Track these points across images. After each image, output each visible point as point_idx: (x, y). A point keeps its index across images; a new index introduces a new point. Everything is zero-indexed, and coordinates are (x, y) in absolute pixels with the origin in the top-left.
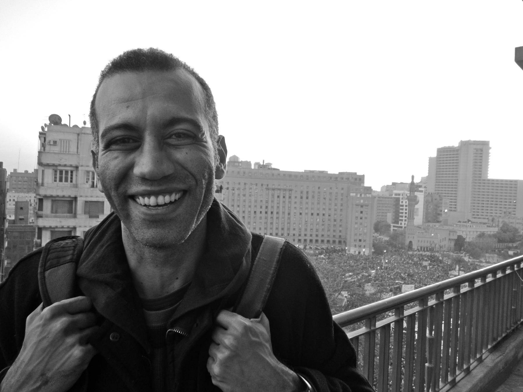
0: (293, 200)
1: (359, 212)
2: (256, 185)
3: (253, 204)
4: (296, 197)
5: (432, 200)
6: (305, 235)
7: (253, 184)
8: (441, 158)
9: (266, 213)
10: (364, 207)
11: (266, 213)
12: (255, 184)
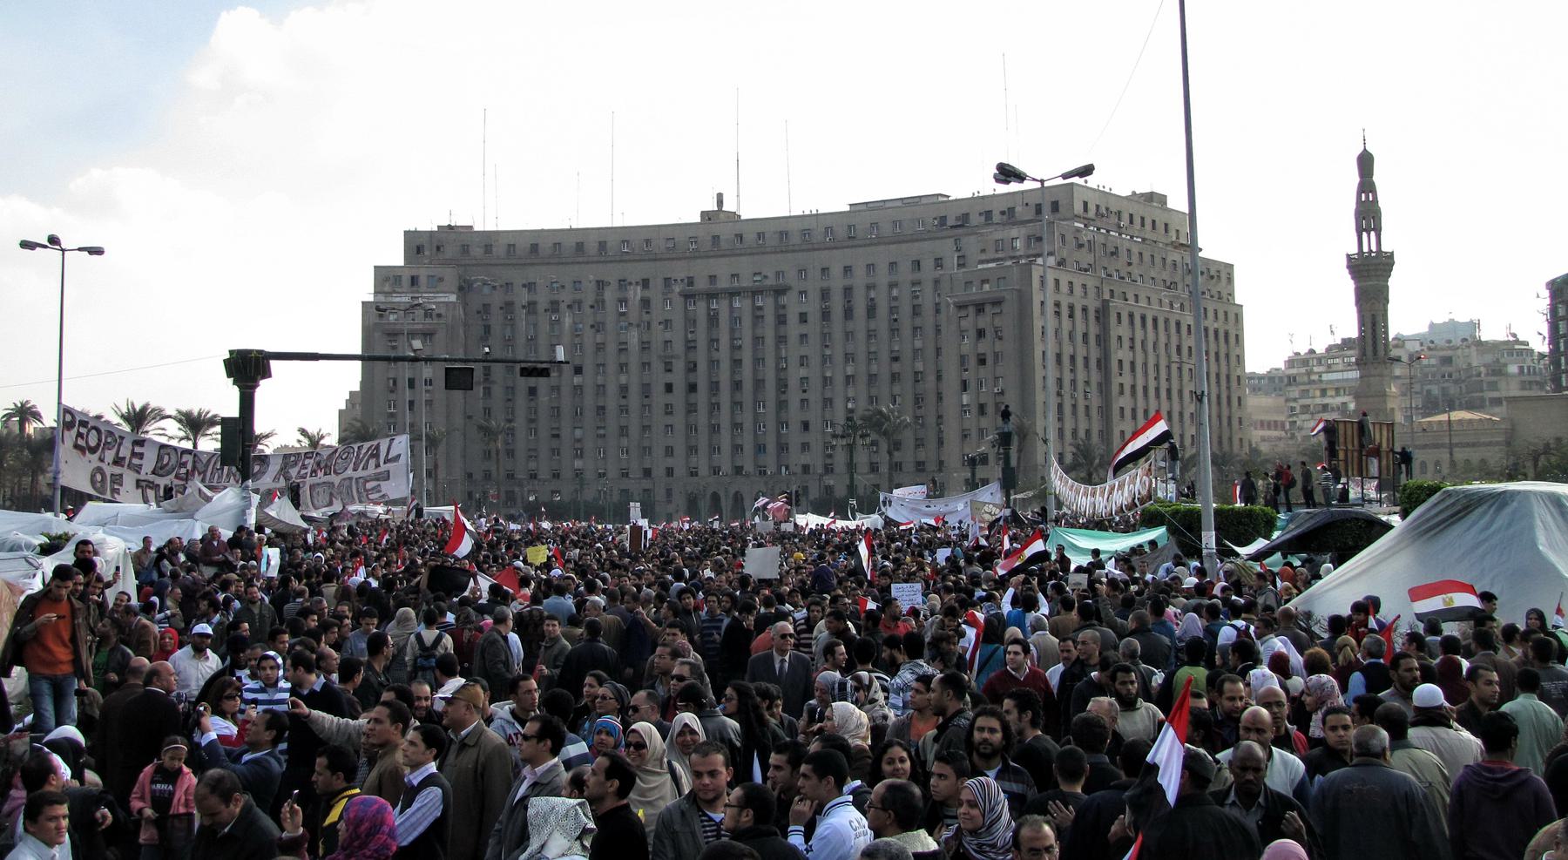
0: (793, 329)
1: (973, 333)
2: (645, 283)
3: (634, 360)
4: (803, 318)
7: (630, 284)
9: (692, 388)
10: (988, 308)
11: (692, 388)
12: (637, 283)
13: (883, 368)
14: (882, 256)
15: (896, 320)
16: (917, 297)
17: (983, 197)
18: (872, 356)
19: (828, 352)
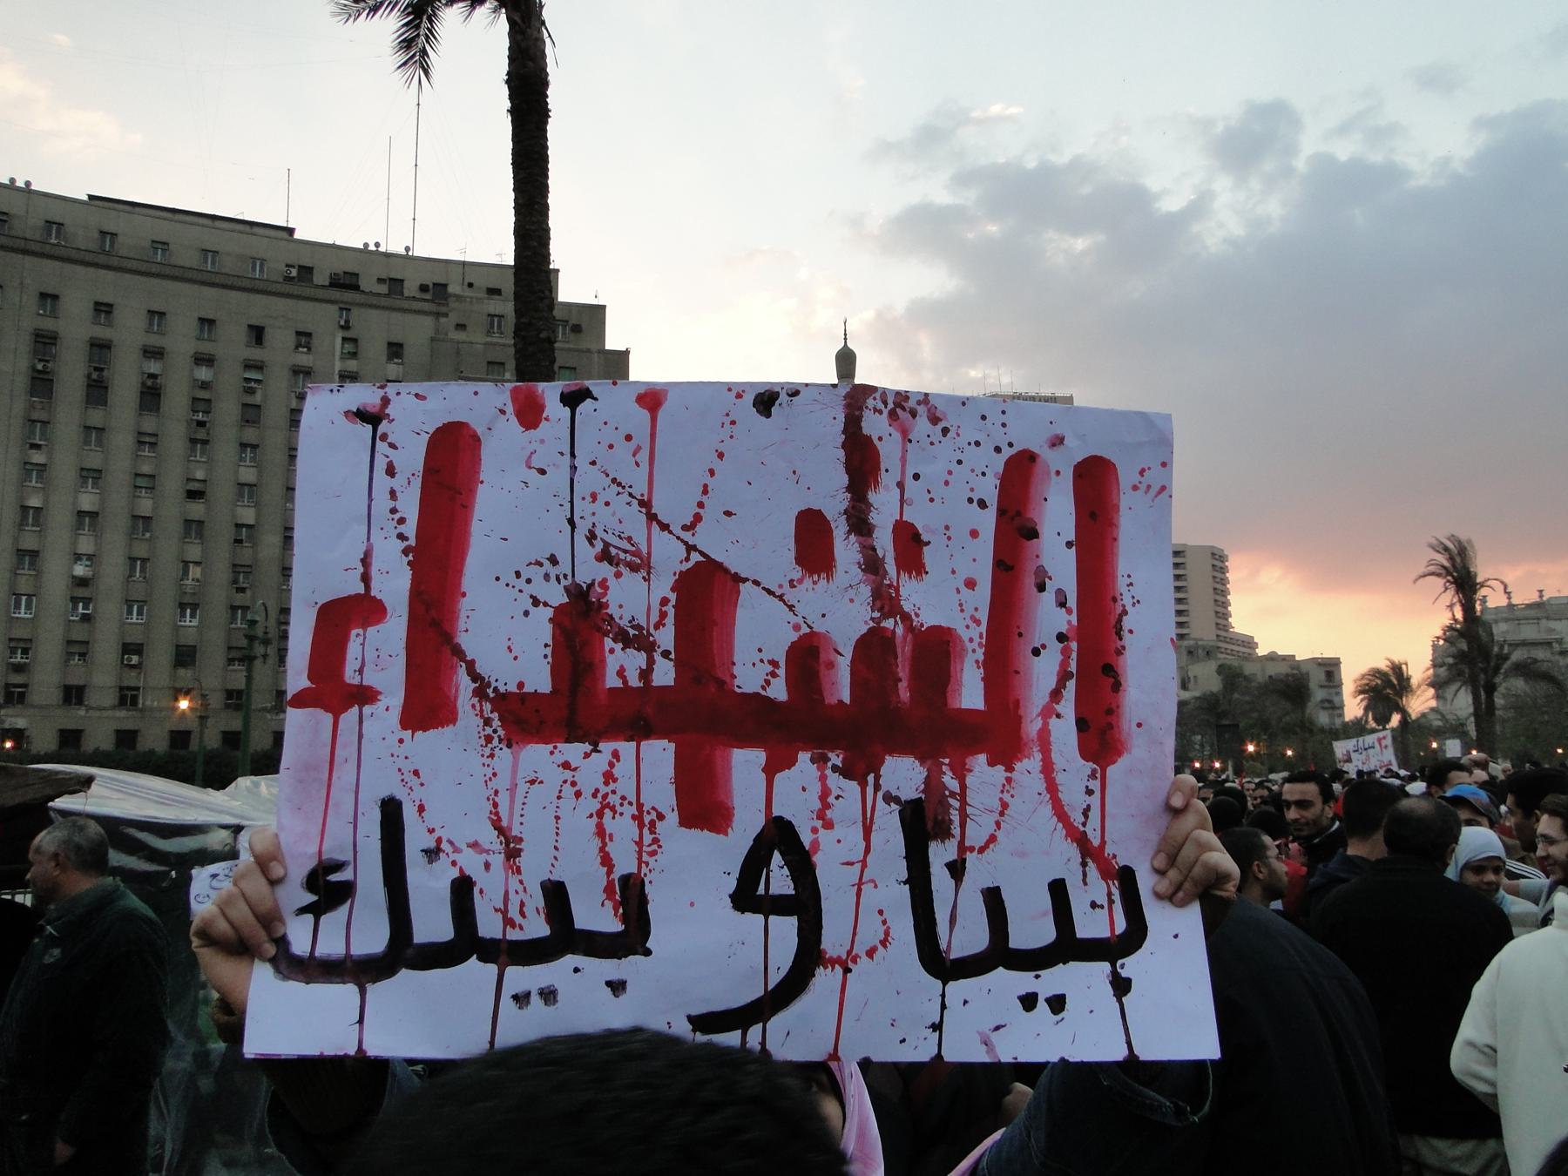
6: (73, 695)
13: (171, 508)
14: (185, 303)
15: (201, 424)
16: (251, 391)
17: (387, 255)
18: (146, 482)
19: (38, 458)
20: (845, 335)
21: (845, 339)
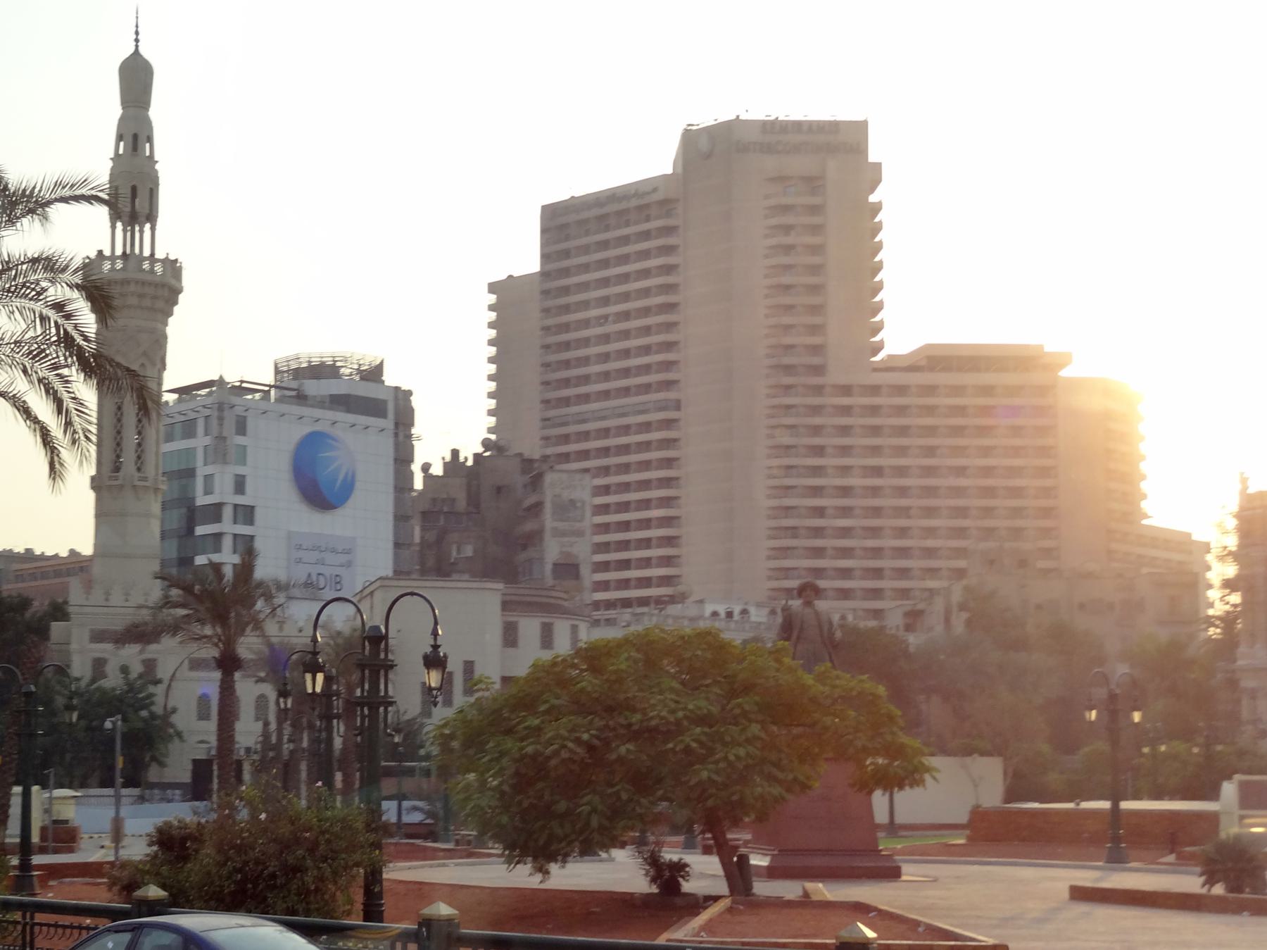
5: (474, 500)
8: (566, 272)
20: (137, 33)
21: (137, 40)
